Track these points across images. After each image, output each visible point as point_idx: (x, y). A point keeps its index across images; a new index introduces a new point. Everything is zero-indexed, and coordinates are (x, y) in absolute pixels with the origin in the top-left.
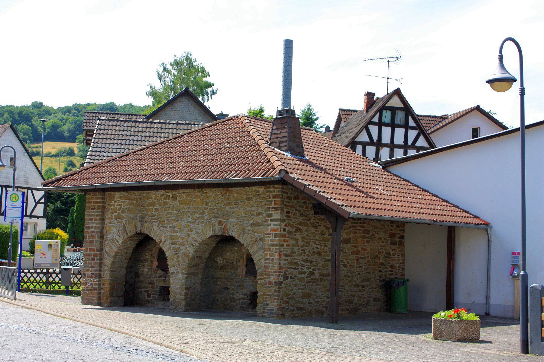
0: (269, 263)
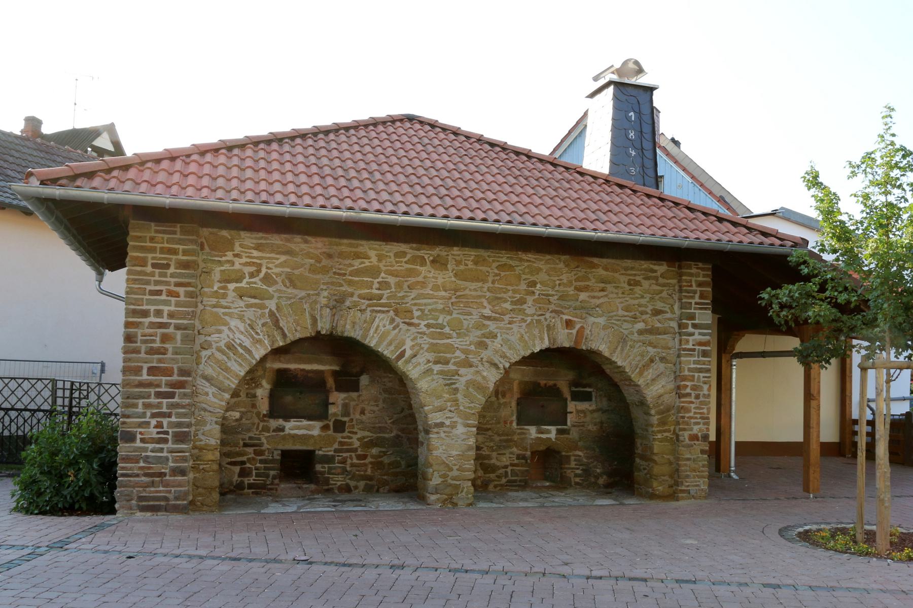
0: (692, 402)
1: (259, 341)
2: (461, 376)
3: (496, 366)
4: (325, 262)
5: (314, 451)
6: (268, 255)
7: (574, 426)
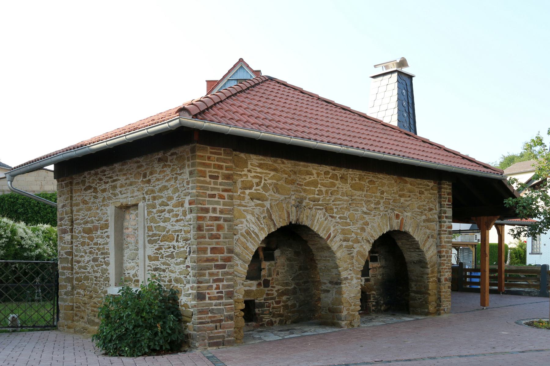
0: (445, 260)
1: (262, 229)
2: (355, 249)
3: (368, 241)
4: (293, 177)
5: (254, 300)
6: (265, 171)
7: (372, 277)
